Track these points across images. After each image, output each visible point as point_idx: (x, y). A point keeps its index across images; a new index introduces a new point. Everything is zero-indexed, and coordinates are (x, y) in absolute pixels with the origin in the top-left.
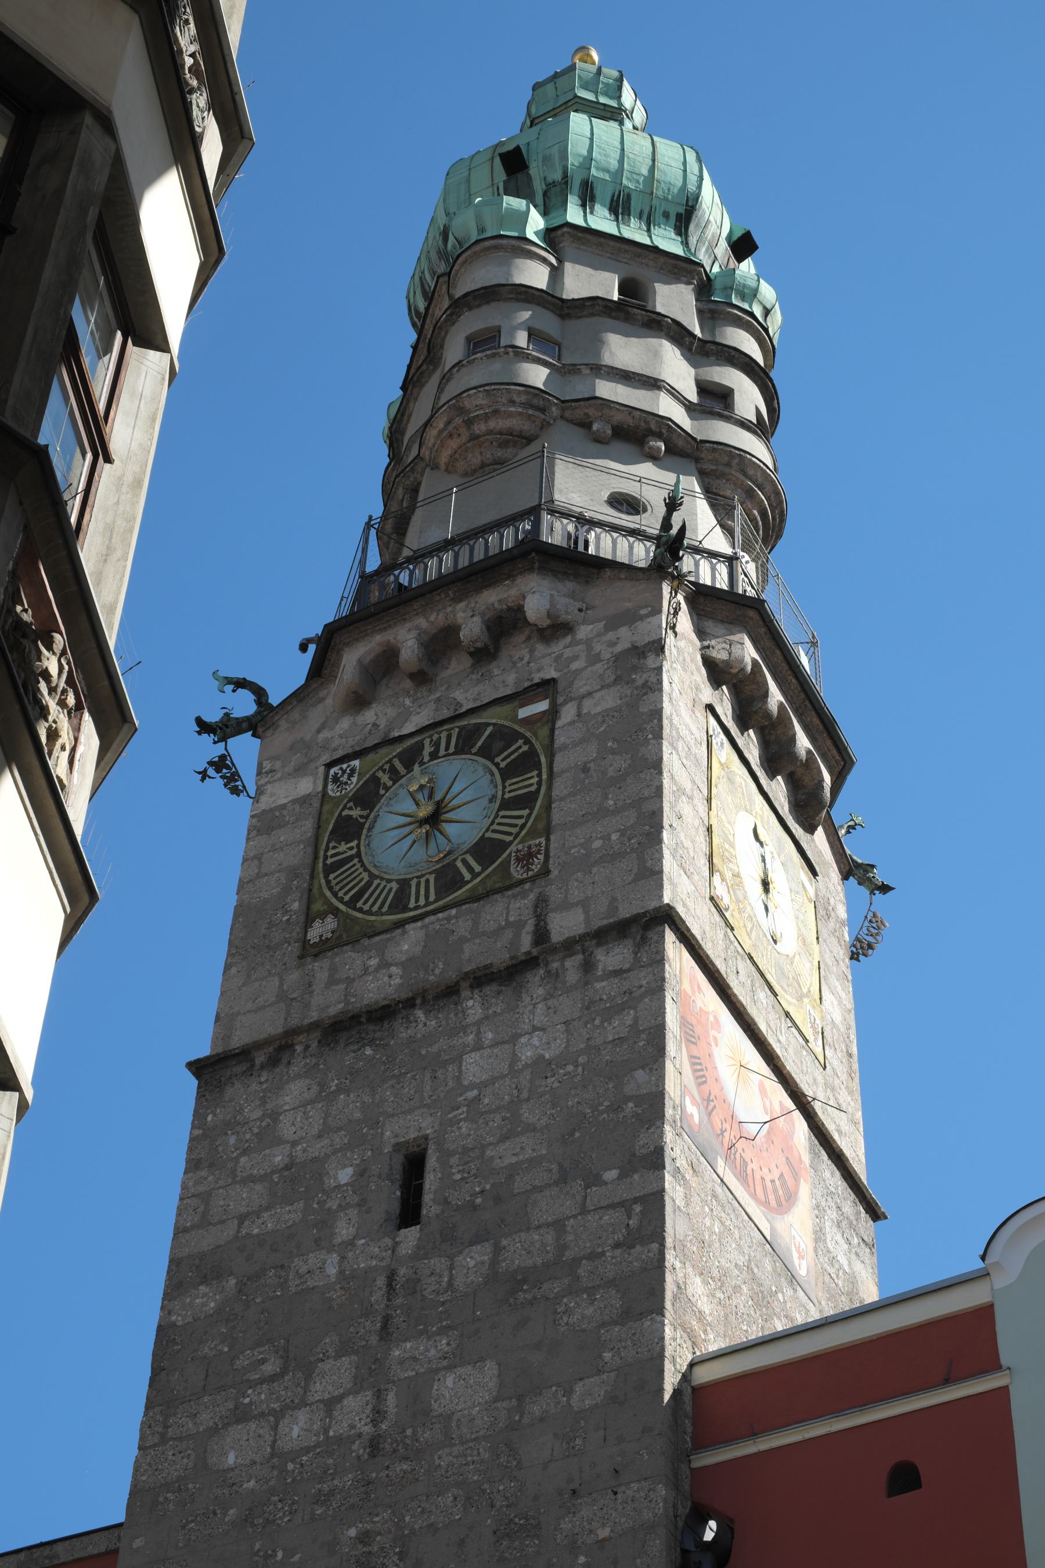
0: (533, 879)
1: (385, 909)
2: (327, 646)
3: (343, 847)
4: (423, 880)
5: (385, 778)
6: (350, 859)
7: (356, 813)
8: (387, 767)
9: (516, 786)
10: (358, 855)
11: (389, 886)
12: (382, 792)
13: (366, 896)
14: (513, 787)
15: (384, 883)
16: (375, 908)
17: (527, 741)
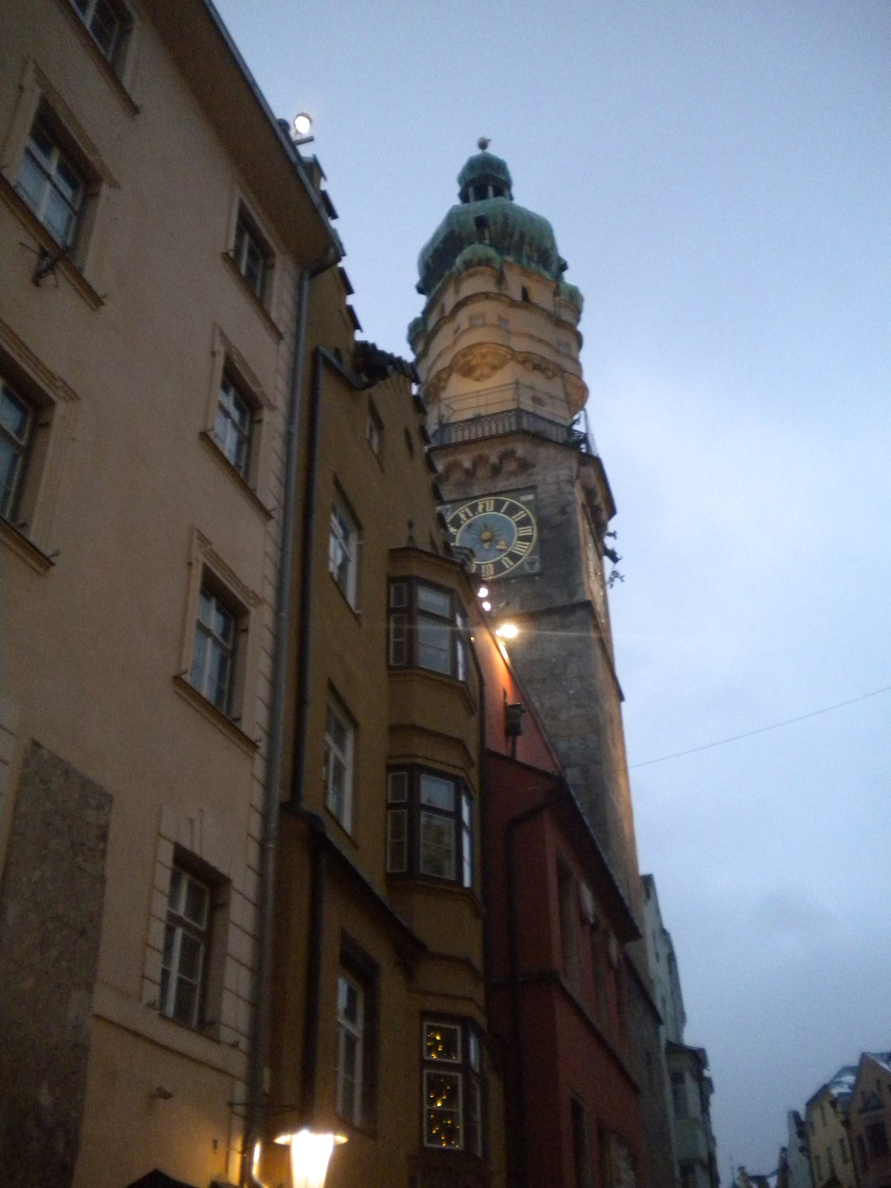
5: (463, 516)
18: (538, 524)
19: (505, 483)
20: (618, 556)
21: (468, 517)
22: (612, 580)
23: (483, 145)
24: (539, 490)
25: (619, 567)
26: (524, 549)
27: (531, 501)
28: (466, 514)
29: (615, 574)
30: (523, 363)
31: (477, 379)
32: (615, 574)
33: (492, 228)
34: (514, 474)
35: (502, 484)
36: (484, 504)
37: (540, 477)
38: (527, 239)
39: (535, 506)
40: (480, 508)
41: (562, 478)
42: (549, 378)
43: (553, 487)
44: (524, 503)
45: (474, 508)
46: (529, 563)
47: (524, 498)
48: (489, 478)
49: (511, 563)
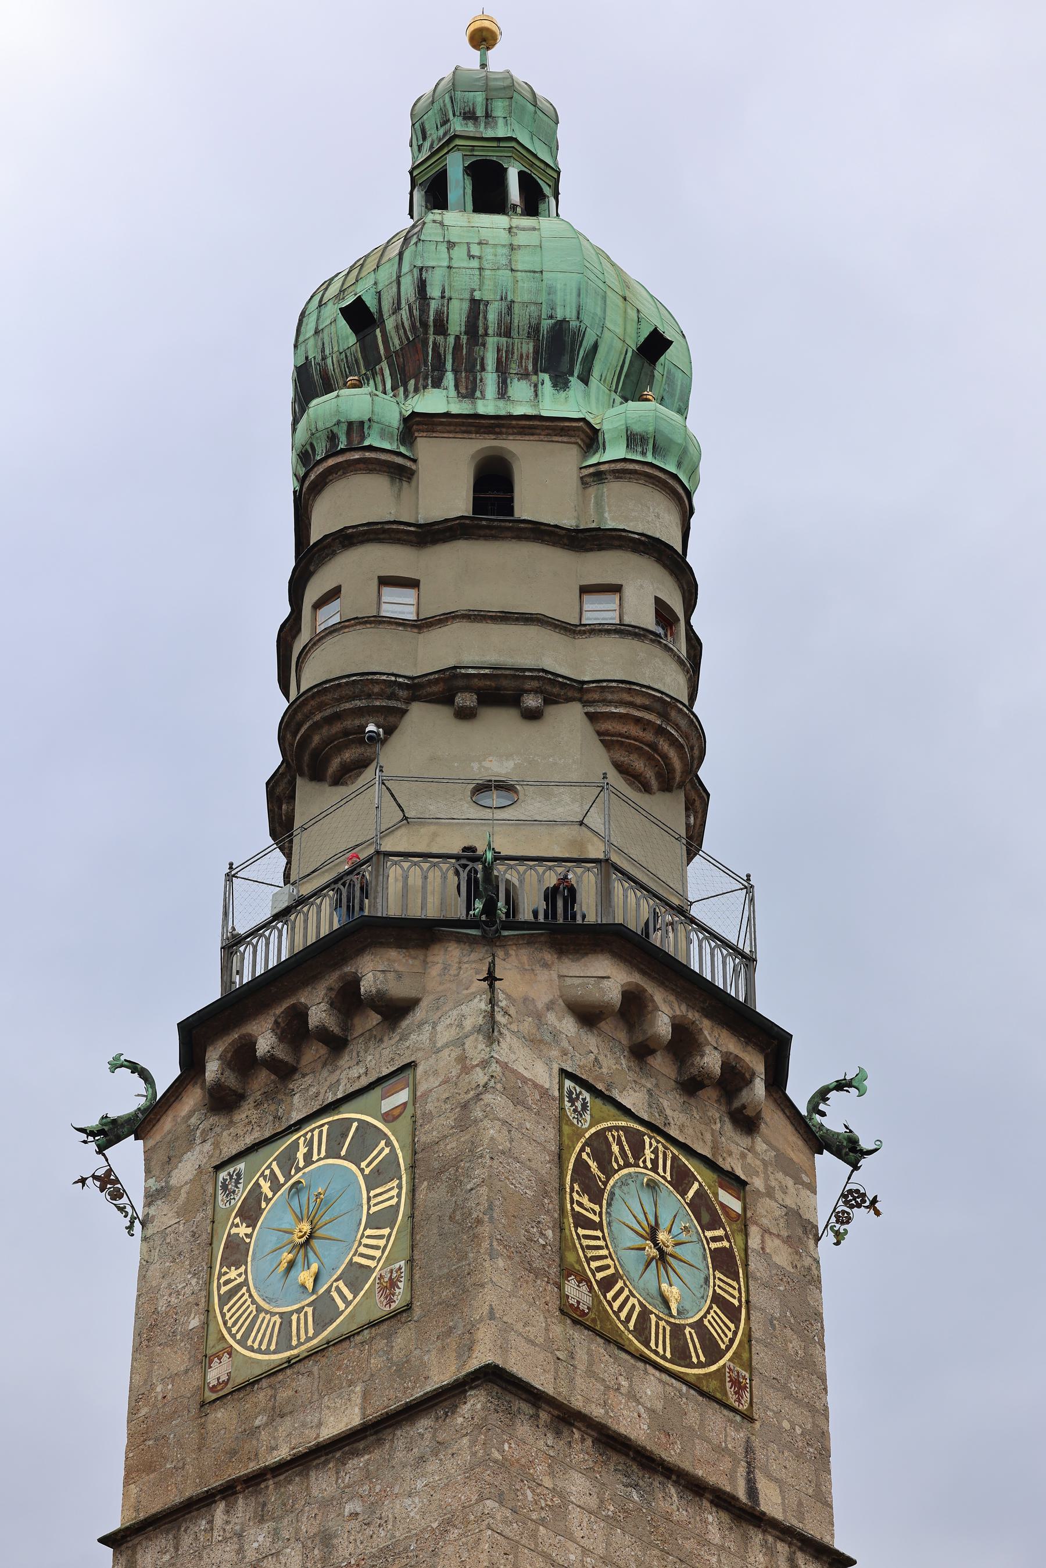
0: (395, 1315)
1: (273, 1347)
2: (195, 1034)
3: (233, 1273)
4: (302, 1315)
5: (266, 1187)
6: (239, 1287)
7: (243, 1230)
8: (267, 1172)
9: (380, 1198)
10: (245, 1283)
11: (273, 1319)
12: (263, 1205)
13: (253, 1334)
14: (380, 1198)
15: (268, 1317)
16: (263, 1347)
17: (389, 1143)
18: (412, 1167)
19: (355, 1072)
20: (865, 1144)
21: (276, 1187)
22: (843, 1219)
23: (483, 39)
24: (420, 1070)
25: (868, 1177)
26: (377, 1250)
27: (405, 1104)
28: (273, 1177)
29: (854, 1198)
30: (446, 699)
31: (338, 781)
32: (854, 1198)
33: (390, 324)
34: (375, 1038)
35: (350, 1073)
36: (310, 1144)
37: (420, 1038)
38: (492, 317)
39: (412, 1118)
40: (303, 1150)
41: (468, 1024)
42: (533, 715)
43: (448, 1056)
44: (389, 1118)
45: (287, 1162)
46: (383, 1288)
47: (388, 1104)
48: (324, 1065)
49: (350, 1297)
